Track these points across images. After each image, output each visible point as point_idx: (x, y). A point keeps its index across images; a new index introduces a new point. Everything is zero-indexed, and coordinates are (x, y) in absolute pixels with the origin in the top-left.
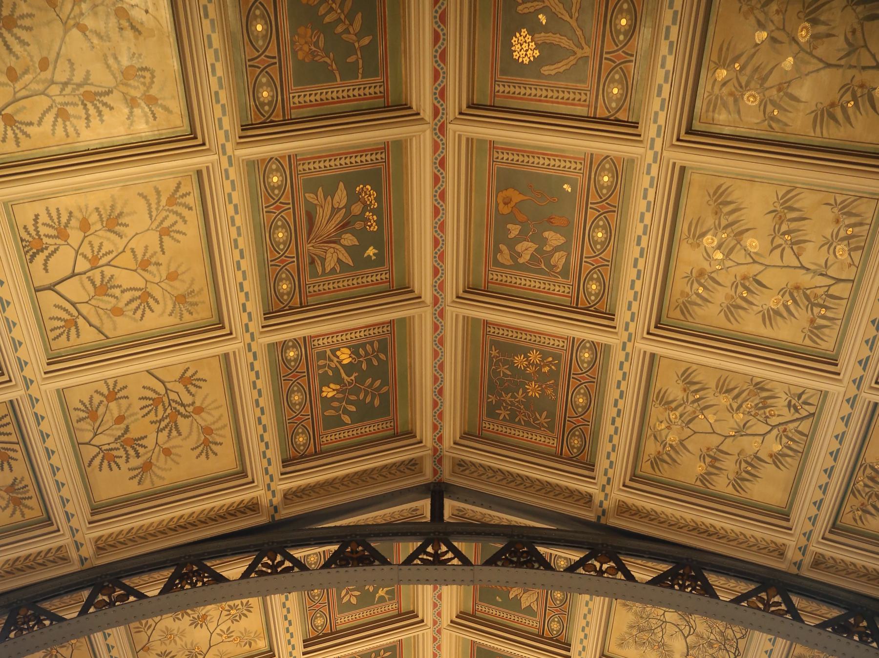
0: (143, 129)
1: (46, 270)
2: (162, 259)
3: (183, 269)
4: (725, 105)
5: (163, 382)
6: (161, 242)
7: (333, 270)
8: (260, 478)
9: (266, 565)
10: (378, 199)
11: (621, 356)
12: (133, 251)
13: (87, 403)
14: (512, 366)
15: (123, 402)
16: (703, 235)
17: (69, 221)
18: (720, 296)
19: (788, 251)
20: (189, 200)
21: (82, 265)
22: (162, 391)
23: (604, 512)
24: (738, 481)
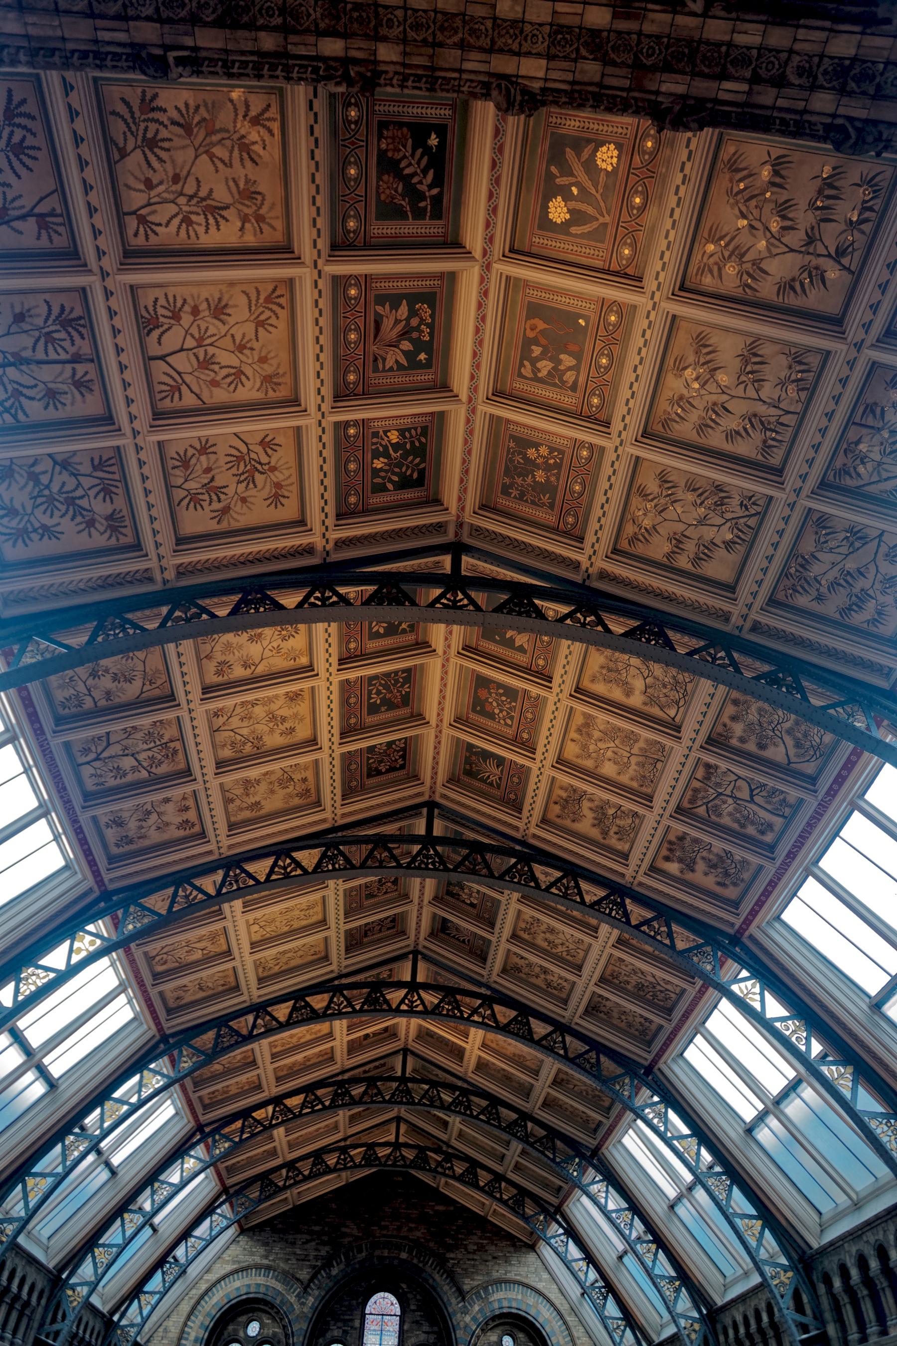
0: (250, 239)
1: (159, 343)
2: (256, 345)
3: (272, 354)
5: (246, 444)
6: (257, 331)
7: (391, 369)
9: (317, 598)
10: (432, 316)
12: (233, 336)
13: (182, 454)
15: (213, 457)
16: (685, 368)
17: (183, 305)
18: (694, 417)
20: (282, 301)
21: (190, 343)
22: (244, 450)
23: (589, 576)
24: (697, 560)
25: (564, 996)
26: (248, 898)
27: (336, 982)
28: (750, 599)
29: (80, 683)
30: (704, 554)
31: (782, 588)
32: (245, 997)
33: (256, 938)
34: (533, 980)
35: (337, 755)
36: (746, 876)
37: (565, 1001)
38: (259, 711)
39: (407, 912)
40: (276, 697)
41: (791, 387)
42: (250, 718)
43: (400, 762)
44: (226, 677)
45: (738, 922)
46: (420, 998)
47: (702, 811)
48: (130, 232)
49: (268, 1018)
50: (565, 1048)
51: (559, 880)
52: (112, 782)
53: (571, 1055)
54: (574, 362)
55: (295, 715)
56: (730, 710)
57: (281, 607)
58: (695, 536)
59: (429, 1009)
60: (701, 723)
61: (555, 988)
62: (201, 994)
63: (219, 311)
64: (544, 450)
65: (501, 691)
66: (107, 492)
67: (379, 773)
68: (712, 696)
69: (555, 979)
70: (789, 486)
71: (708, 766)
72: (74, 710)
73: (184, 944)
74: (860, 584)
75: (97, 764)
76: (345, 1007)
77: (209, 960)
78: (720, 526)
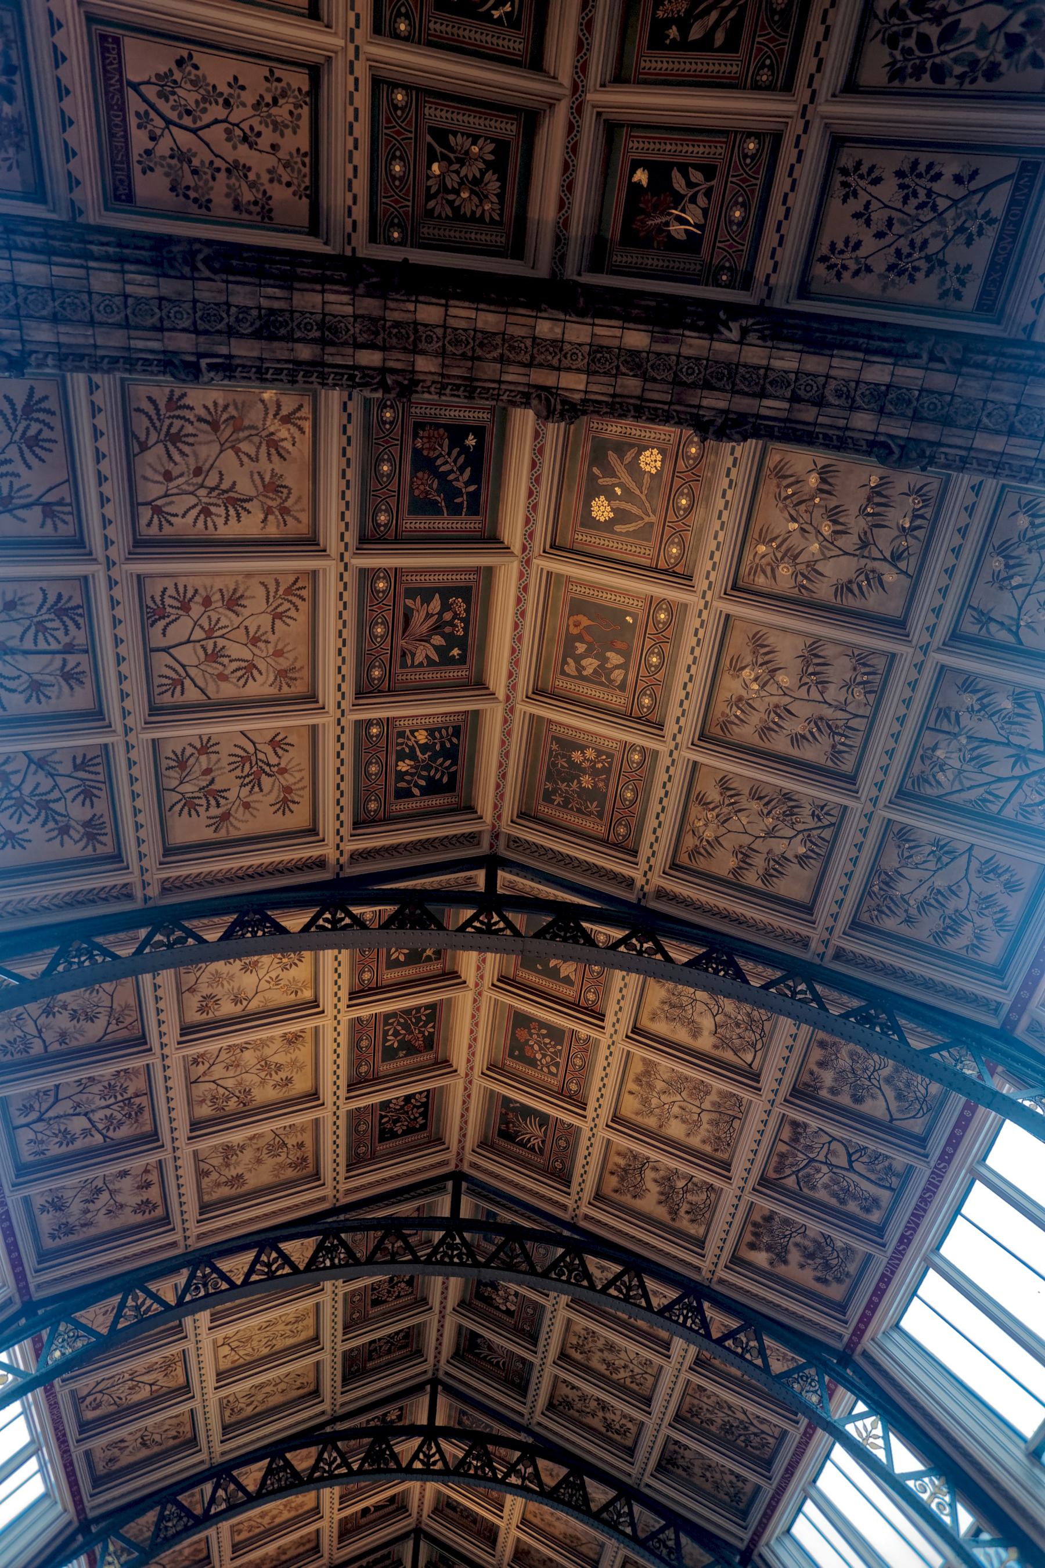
0: (272, 530)
1: (164, 634)
2: (272, 638)
4: (764, 572)
5: (254, 743)
7: (421, 664)
8: (331, 838)
11: (668, 761)
12: (246, 628)
13: (179, 754)
14: (570, 761)
15: (214, 757)
16: (743, 668)
17: (194, 596)
18: (755, 719)
19: (813, 689)
20: (304, 593)
21: (198, 634)
22: (251, 750)
24: (767, 876)
25: (629, 1443)
26: (219, 1308)
27: (328, 1429)
28: (830, 923)
29: (31, 1023)
30: (775, 870)
31: (865, 908)
32: (203, 1456)
33: (225, 1365)
34: (589, 1420)
35: (342, 1113)
36: (852, 1268)
37: (631, 1451)
38: (249, 1057)
39: (425, 1323)
40: (272, 1039)
41: (858, 691)
42: (238, 1066)
43: (421, 1121)
44: (211, 1015)
45: (847, 1333)
46: (439, 1450)
47: (791, 1182)
48: (144, 521)
49: (232, 1487)
50: (633, 1524)
51: (618, 1277)
52: (55, 1150)
53: (642, 1535)
54: (621, 660)
55: (294, 1062)
56: (817, 1054)
57: (284, 931)
58: (764, 850)
59: (451, 1467)
60: (783, 1071)
61: (618, 1432)
62: (145, 1453)
63: (234, 602)
64: (590, 754)
65: (544, 1031)
66: (88, 795)
67: (394, 1135)
68: (794, 1037)
69: (617, 1418)
70: (864, 795)
71: (795, 1124)
72: (17, 1056)
73: (127, 1376)
74: (953, 904)
75: (39, 1127)
76: (338, 1467)
77: (159, 1399)
78: (791, 838)
